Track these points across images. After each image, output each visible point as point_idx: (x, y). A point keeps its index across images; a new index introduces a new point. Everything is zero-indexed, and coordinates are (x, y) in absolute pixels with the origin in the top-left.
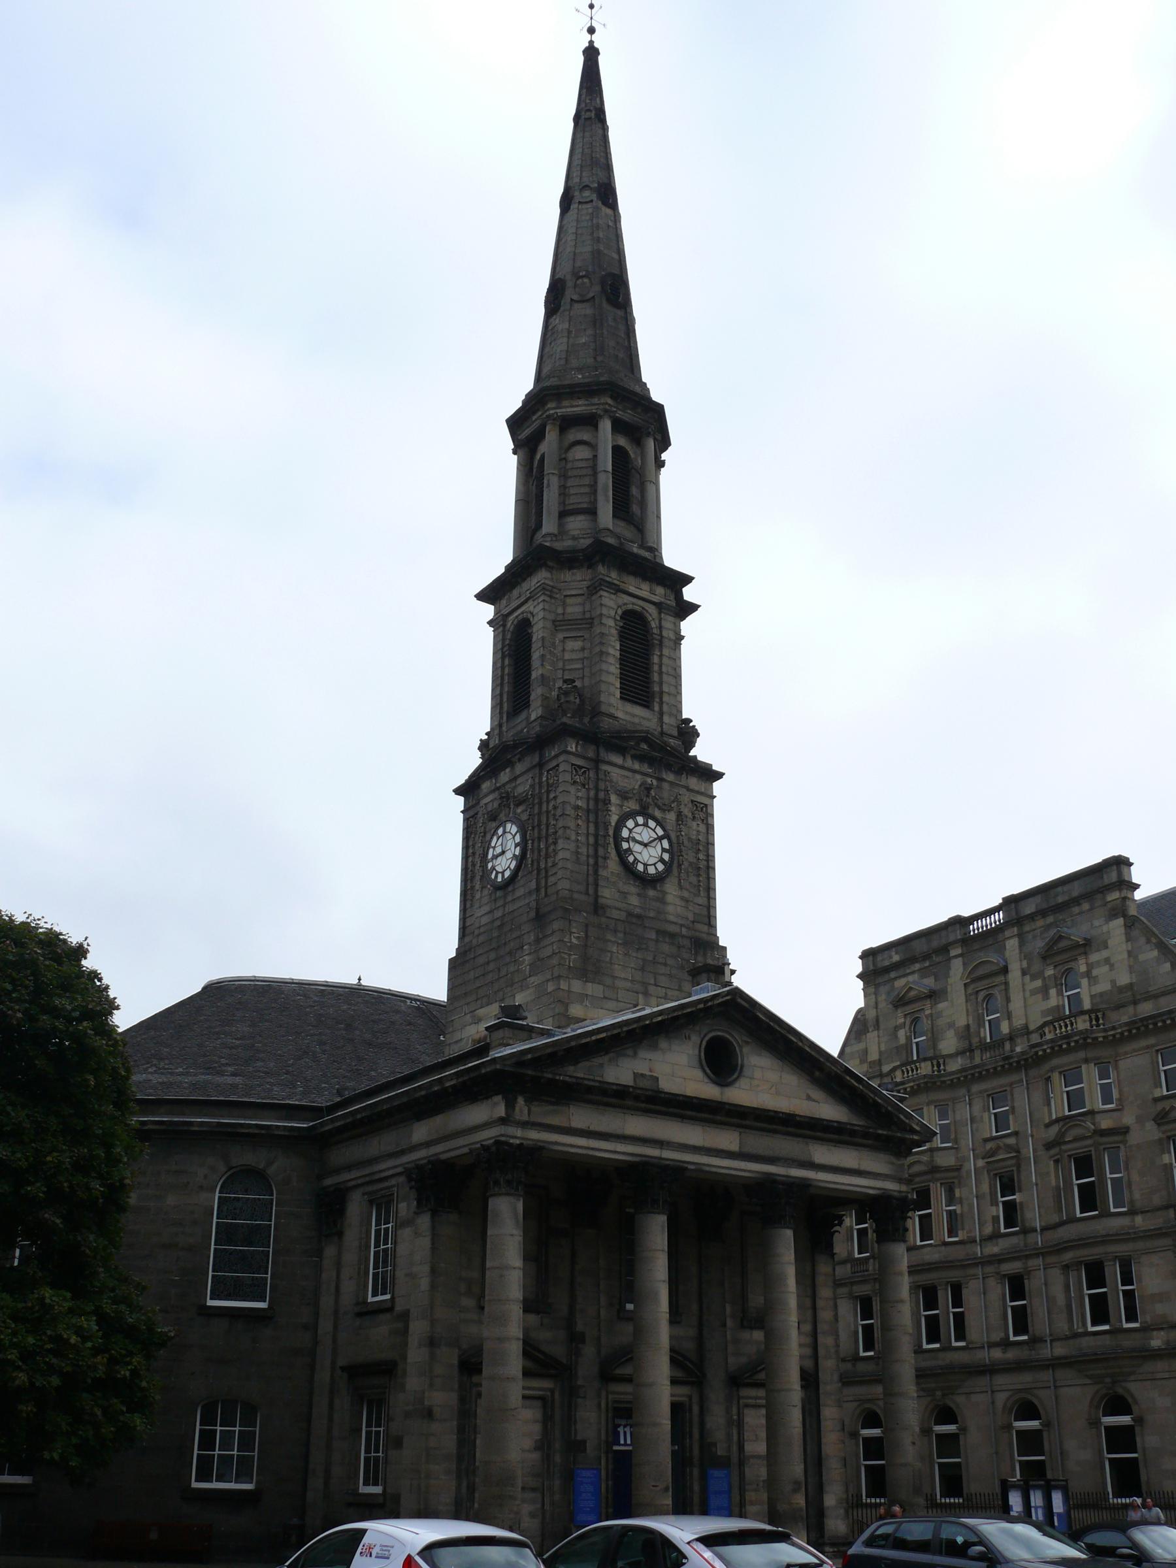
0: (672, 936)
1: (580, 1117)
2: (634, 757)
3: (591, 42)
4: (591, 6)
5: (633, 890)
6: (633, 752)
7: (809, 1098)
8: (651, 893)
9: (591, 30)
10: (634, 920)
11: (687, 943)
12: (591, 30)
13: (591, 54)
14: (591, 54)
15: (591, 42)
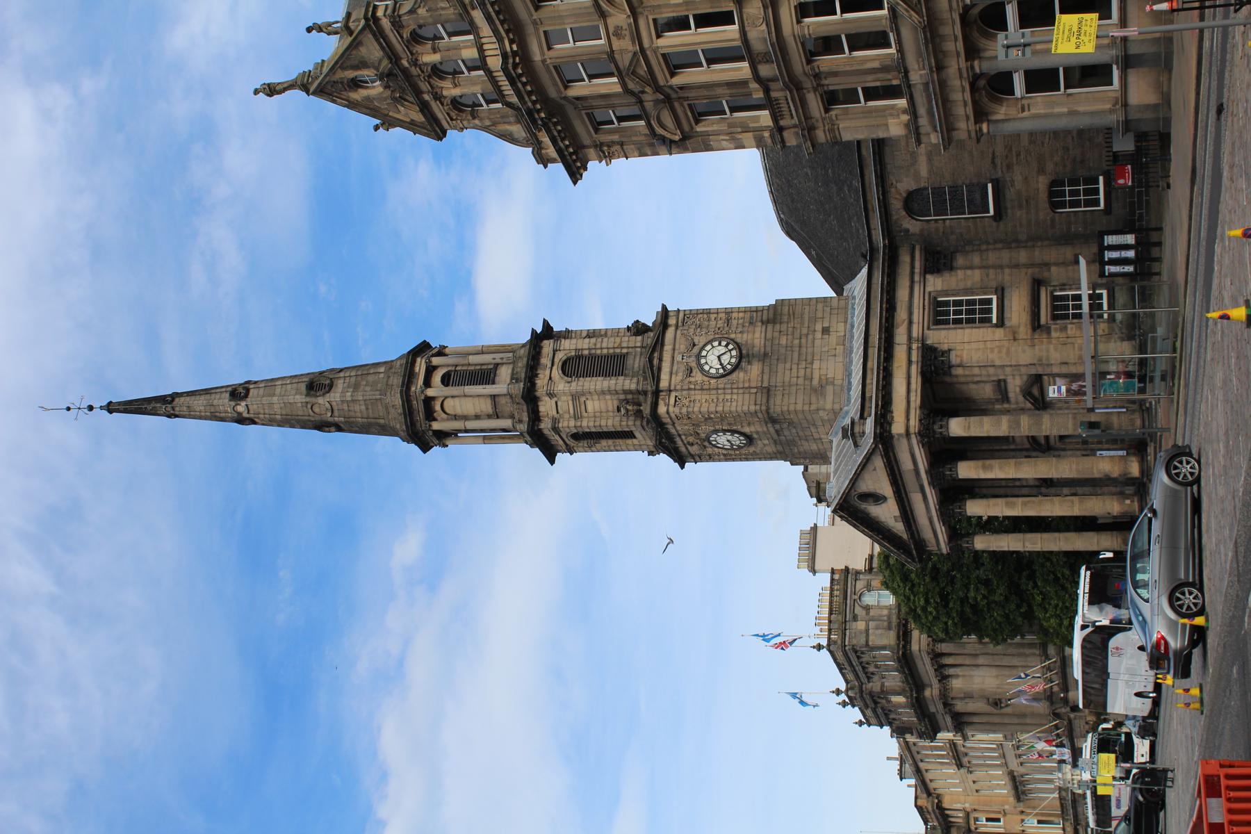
0: (777, 431)
1: (927, 534)
2: (675, 443)
3: (101, 408)
4: (68, 409)
5: (759, 442)
6: (672, 445)
7: (875, 470)
8: (755, 436)
9: (91, 408)
10: (778, 442)
11: (777, 426)
12: (91, 408)
13: (111, 408)
14: (111, 408)
15: (101, 408)
